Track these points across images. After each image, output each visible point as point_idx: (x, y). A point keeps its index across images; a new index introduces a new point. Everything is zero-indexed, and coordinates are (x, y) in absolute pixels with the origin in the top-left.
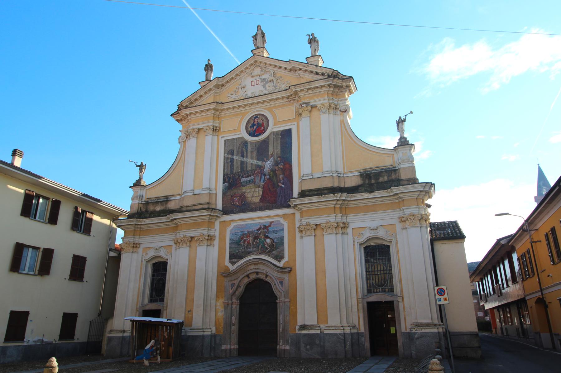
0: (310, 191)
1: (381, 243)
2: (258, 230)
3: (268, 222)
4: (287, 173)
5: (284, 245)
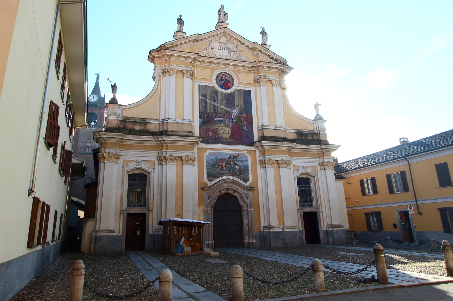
0: (270, 137)
1: (305, 177)
2: (229, 158)
3: (236, 153)
4: (249, 121)
5: (249, 172)
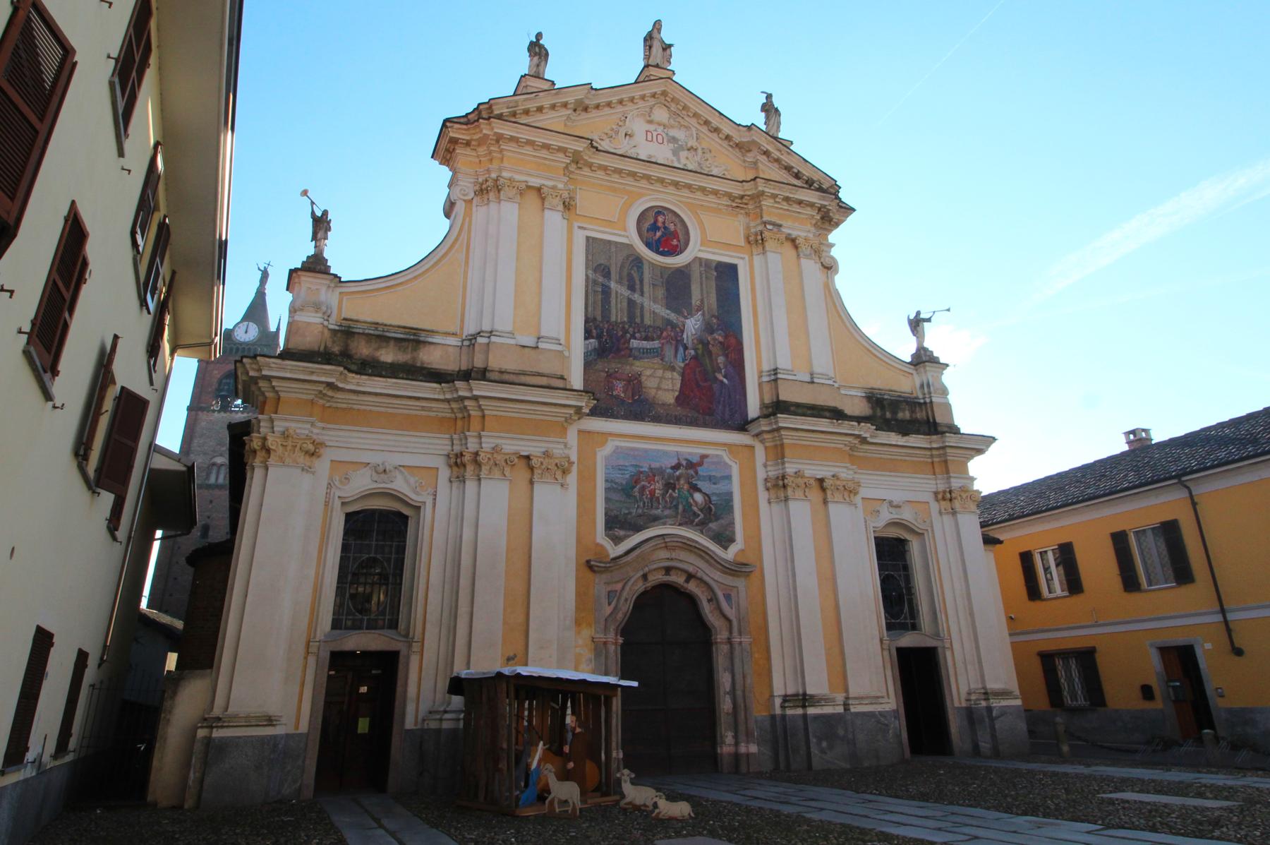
0: (798, 405)
5: (733, 512)
